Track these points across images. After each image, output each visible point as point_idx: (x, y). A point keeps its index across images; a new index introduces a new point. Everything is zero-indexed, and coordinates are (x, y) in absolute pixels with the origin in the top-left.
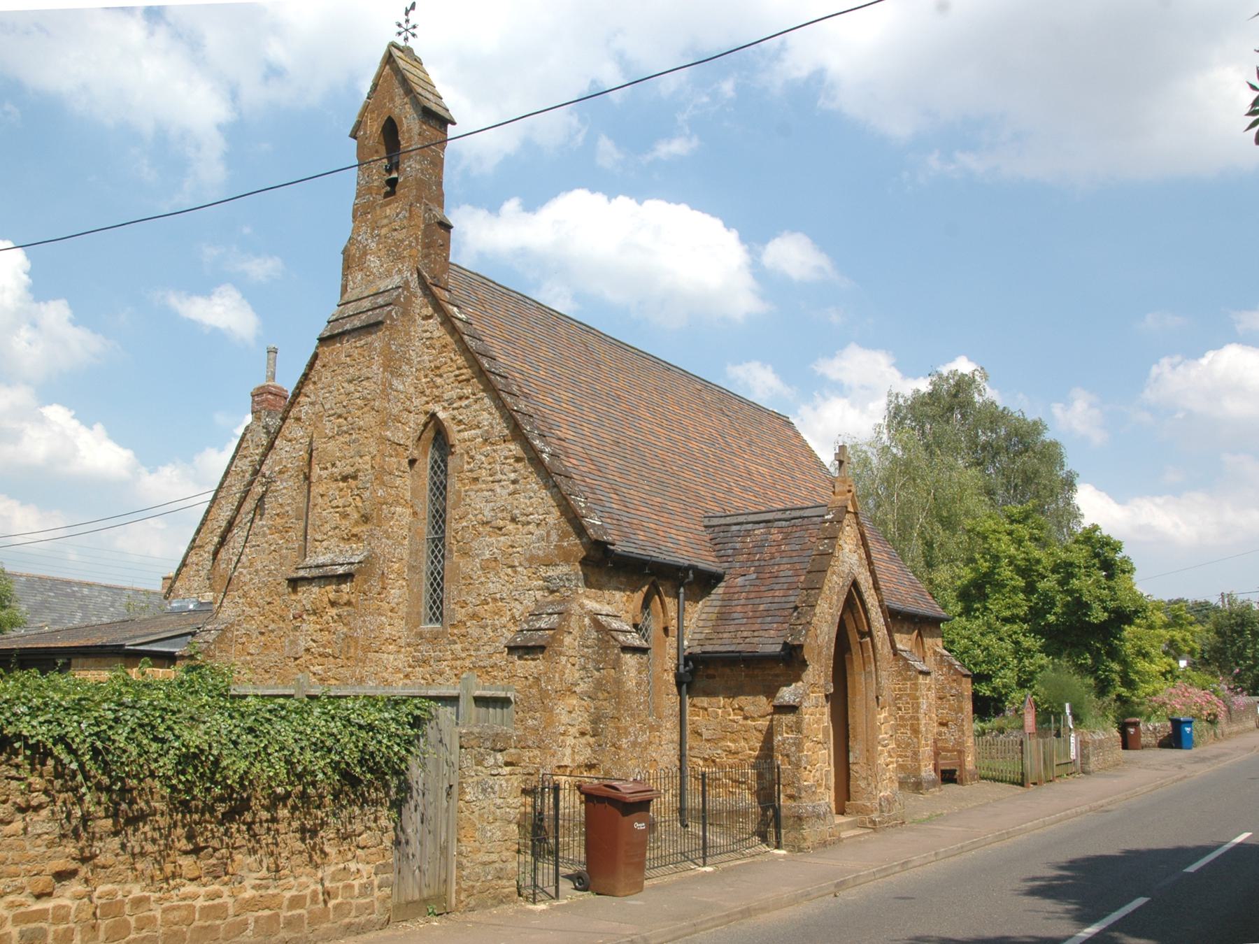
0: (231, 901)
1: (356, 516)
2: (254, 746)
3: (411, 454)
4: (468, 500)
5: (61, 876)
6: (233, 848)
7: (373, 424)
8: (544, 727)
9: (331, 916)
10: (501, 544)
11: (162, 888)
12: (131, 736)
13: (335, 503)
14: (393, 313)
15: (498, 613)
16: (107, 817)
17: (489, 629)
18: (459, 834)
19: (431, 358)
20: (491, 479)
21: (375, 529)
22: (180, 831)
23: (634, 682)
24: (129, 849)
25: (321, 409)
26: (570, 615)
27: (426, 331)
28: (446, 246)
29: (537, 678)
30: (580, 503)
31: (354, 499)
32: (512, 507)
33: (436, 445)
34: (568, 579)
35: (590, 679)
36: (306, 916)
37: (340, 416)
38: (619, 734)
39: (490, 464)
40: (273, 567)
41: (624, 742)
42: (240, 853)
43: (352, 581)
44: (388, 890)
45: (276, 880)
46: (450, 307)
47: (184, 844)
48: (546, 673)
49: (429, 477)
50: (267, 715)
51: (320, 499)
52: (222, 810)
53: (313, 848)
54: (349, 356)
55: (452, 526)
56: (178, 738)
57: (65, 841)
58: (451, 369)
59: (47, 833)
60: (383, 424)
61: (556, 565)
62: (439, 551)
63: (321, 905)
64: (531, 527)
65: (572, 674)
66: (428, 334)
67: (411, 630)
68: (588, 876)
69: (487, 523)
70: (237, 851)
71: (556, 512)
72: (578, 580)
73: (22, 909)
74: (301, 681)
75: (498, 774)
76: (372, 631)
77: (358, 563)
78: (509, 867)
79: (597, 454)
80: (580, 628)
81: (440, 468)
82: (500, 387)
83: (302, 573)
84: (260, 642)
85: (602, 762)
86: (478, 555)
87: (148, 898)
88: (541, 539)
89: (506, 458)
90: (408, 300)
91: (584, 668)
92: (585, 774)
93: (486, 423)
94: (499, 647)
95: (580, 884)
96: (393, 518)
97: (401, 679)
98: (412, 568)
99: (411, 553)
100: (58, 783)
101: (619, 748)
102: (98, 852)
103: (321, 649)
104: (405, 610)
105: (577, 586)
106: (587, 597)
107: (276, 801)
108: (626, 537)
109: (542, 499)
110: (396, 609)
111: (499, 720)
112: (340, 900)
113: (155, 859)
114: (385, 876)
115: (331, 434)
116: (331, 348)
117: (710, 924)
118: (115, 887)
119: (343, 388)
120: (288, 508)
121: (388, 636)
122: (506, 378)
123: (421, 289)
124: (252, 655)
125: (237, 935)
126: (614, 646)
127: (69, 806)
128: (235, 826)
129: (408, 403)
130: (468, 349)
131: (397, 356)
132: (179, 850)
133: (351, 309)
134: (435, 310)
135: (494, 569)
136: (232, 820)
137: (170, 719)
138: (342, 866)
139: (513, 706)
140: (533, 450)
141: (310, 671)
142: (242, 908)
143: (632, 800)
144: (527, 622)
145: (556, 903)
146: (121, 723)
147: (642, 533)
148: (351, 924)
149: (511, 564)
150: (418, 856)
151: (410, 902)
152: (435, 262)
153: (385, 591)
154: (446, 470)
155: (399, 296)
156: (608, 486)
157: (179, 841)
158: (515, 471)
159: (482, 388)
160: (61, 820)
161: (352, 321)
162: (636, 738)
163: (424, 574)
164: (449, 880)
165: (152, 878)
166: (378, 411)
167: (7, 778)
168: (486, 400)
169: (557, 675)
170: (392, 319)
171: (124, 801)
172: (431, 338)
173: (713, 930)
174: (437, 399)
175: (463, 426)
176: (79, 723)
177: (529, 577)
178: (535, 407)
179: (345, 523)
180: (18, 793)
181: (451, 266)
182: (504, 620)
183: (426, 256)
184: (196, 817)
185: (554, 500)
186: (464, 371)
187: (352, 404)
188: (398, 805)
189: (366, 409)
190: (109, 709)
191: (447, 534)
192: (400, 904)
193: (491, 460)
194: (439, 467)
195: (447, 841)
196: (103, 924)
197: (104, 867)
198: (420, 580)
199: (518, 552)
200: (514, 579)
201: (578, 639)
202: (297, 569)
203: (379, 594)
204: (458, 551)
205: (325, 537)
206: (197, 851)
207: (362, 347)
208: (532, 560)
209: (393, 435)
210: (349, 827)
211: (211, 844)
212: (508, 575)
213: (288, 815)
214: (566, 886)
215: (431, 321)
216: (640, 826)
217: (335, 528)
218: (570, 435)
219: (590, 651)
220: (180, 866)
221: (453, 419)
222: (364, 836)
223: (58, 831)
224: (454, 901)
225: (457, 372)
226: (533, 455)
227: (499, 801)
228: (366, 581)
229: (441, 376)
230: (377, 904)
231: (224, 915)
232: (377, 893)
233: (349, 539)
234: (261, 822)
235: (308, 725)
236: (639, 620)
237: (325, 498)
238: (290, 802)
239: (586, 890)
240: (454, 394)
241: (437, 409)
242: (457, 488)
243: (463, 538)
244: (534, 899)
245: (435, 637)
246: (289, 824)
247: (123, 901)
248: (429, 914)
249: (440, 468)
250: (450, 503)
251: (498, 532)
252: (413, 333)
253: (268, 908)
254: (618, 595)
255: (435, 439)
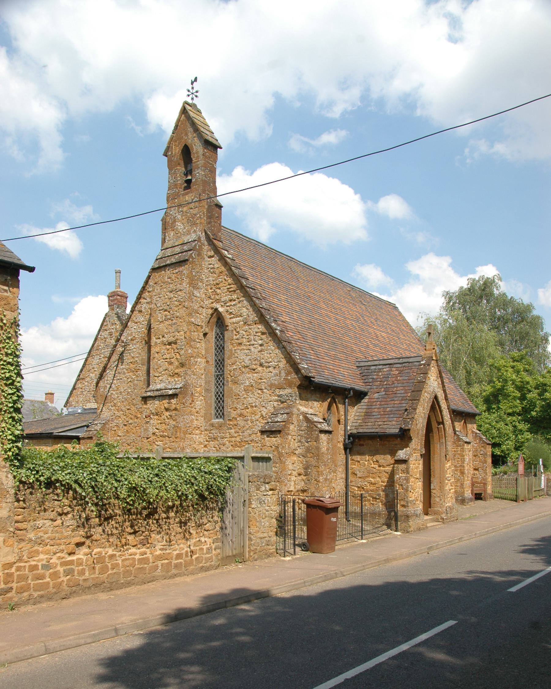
0: (151, 556)
1: (177, 363)
2: (159, 483)
3: (204, 330)
4: (236, 354)
5: (79, 545)
6: (150, 531)
7: (184, 315)
8: (281, 472)
9: (194, 563)
10: (255, 378)
11: (121, 550)
12: (106, 479)
13: (165, 357)
14: (193, 255)
15: (254, 413)
16: (96, 517)
17: (249, 422)
18: (249, 524)
19: (214, 279)
20: (249, 343)
21: (187, 371)
22: (127, 524)
23: (326, 448)
24: (106, 532)
25: (155, 307)
26: (293, 414)
27: (211, 264)
28: (219, 217)
29: (277, 447)
30: (297, 357)
31: (176, 355)
32: (260, 358)
33: (218, 325)
34: (291, 396)
35: (303, 447)
36: (183, 563)
37: (166, 310)
38: (318, 474)
39: (248, 335)
40: (130, 390)
41: (321, 479)
42: (154, 533)
43: (177, 398)
44: (218, 551)
45: (169, 546)
46: (223, 251)
47: (129, 530)
48: (281, 444)
49: (214, 342)
50: (163, 468)
51: (156, 355)
52: (146, 513)
53: (185, 531)
54: (170, 278)
55: (228, 368)
56: (126, 480)
57: (79, 529)
58: (225, 285)
59: (71, 525)
60: (190, 315)
61: (285, 388)
62: (221, 381)
63: (190, 558)
64: (271, 369)
65: (294, 444)
66: (212, 266)
67: (207, 423)
68: (308, 544)
69: (247, 367)
70: (152, 533)
71: (284, 361)
72: (296, 396)
73: (64, 560)
74: (159, 450)
75: (267, 495)
76: (187, 423)
77: (180, 388)
78: (272, 540)
79: (302, 329)
80: (298, 421)
81: (220, 337)
82: (252, 295)
83: (149, 394)
84: (124, 429)
85: (310, 489)
86: (242, 384)
87: (115, 555)
88: (276, 375)
89: (256, 333)
90: (201, 248)
91: (300, 441)
92: (301, 494)
93: (245, 314)
94: (254, 431)
95: (304, 548)
96: (196, 364)
97: (202, 448)
98: (207, 390)
99: (206, 383)
100: (75, 502)
101: (319, 481)
102: (93, 534)
103: (161, 433)
104: (204, 412)
105: (296, 400)
106: (301, 405)
107: (169, 508)
108: (318, 373)
109: (276, 354)
110: (199, 412)
111: (265, 468)
112: (198, 555)
113: (118, 536)
114: (217, 544)
115: (161, 320)
116: (159, 274)
117: (371, 566)
118: (101, 549)
119: (167, 295)
120: (137, 359)
121: (195, 426)
122: (255, 289)
123: (207, 241)
124: (120, 436)
125: (154, 572)
126: (316, 430)
127: (80, 512)
128: (151, 521)
129: (202, 303)
130: (235, 275)
131: (196, 278)
132: (128, 532)
133: (169, 252)
134: (215, 253)
135: (251, 390)
136: (149, 518)
137: (122, 471)
138: (198, 539)
139: (272, 462)
140: (271, 328)
141: (156, 445)
142: (156, 559)
143: (330, 507)
144: (270, 418)
145: (294, 557)
146: (100, 473)
147: (326, 371)
148: (203, 567)
149: (260, 388)
150: (231, 534)
151: (228, 557)
152: (214, 226)
153: (193, 402)
154: (224, 339)
155: (195, 245)
156: (308, 346)
157: (127, 528)
158: (261, 340)
159: (242, 295)
160: (77, 519)
161: (170, 259)
162: (327, 476)
163: (213, 393)
164: (245, 546)
165: (117, 545)
166: (187, 308)
167: (53, 500)
168: (245, 302)
169: (287, 445)
170: (193, 258)
171: (103, 510)
172: (213, 268)
173: (372, 568)
174: (218, 301)
175: (233, 316)
176: (83, 474)
177: (270, 395)
178: (269, 304)
179: (171, 367)
180: (58, 507)
181: (222, 228)
182: (257, 417)
183: (209, 223)
184: (134, 517)
185: (283, 355)
186: (232, 286)
187: (172, 304)
188: (222, 510)
189: (180, 307)
190: (94, 467)
191: (225, 373)
192: (224, 557)
193: (248, 334)
194: (220, 337)
195: (243, 527)
196: (98, 567)
197: (96, 541)
198: (211, 396)
199: (264, 382)
200: (262, 396)
201: (297, 426)
202: (146, 391)
203: (191, 404)
204: (232, 381)
205: (160, 375)
206: (135, 533)
207: (177, 273)
208: (271, 386)
209: (195, 321)
210: (201, 521)
211: (141, 529)
212: (259, 394)
213: (174, 515)
214: (298, 549)
215: (213, 259)
216: (334, 520)
217: (166, 370)
218: (287, 319)
219: (303, 432)
220: (128, 540)
221: (227, 312)
222: (208, 525)
223: (76, 524)
224: (247, 556)
225: (228, 287)
226: (271, 331)
227: (267, 508)
228: (184, 398)
229: (219, 289)
230: (214, 557)
231: (148, 563)
232: (214, 552)
233: (173, 376)
234: (162, 519)
235: (182, 472)
236: (326, 416)
237: (159, 354)
238: (175, 509)
239: (307, 551)
240: (227, 298)
241: (218, 306)
242: (230, 348)
243: (234, 375)
244: (284, 555)
245: (220, 426)
246: (175, 520)
247: (105, 556)
248: (237, 562)
249: (220, 337)
250: (226, 356)
251: (253, 371)
252: (203, 265)
253: (167, 559)
254: (316, 403)
255: (217, 322)
